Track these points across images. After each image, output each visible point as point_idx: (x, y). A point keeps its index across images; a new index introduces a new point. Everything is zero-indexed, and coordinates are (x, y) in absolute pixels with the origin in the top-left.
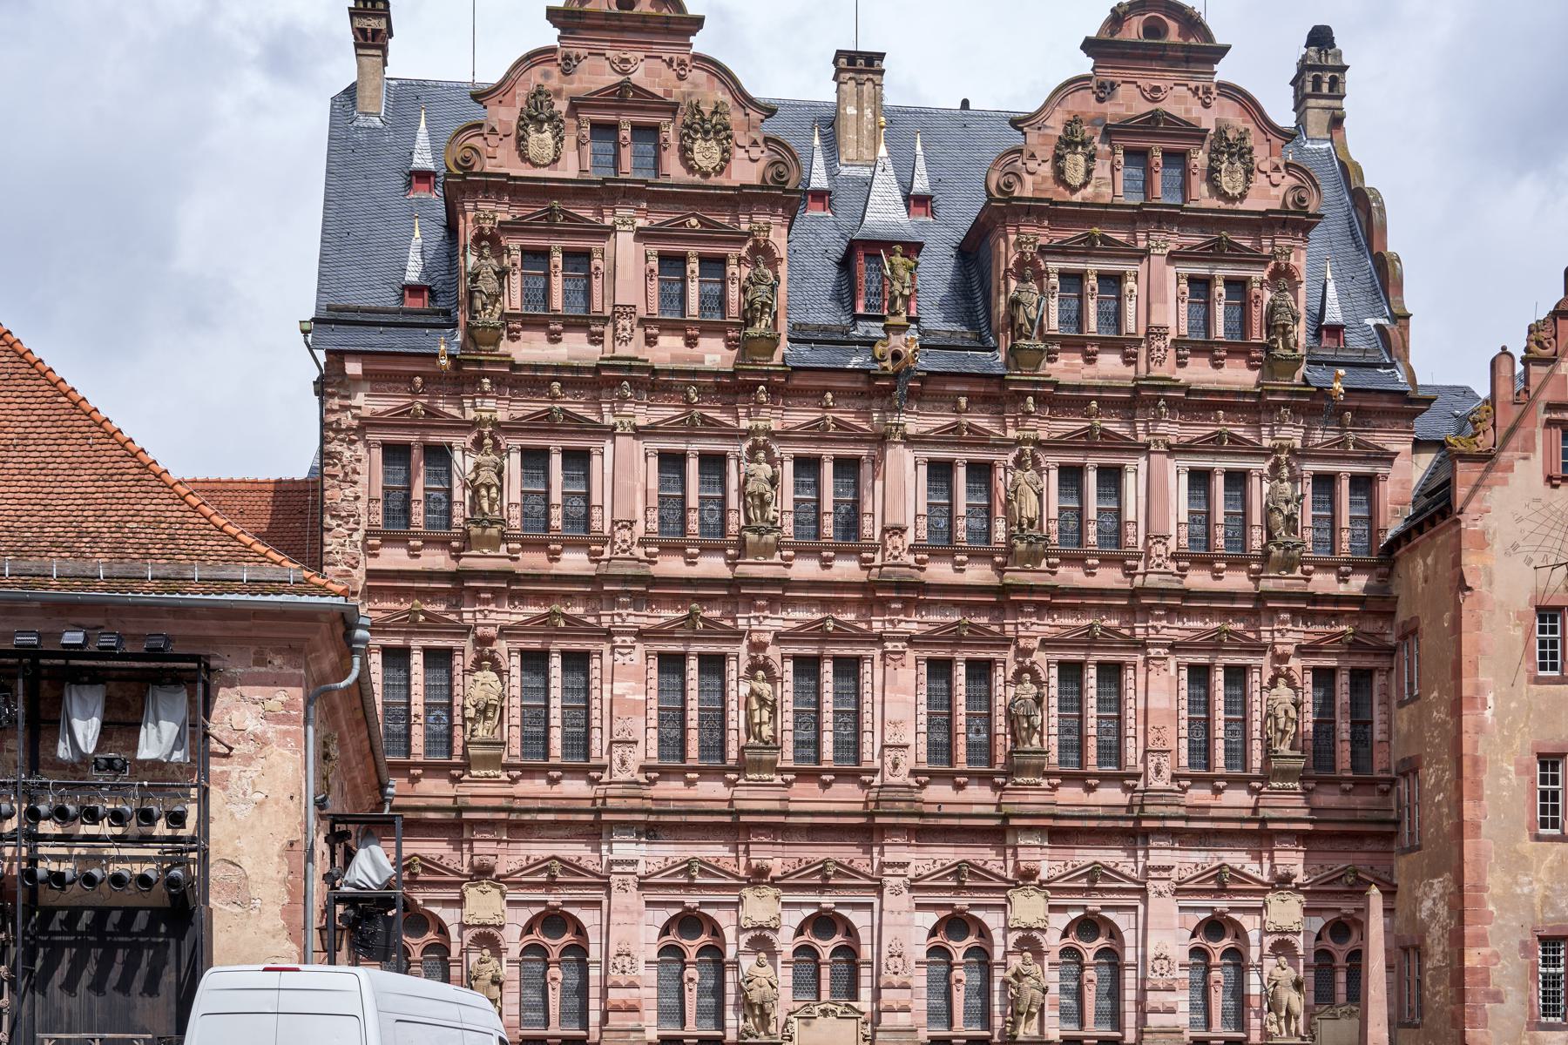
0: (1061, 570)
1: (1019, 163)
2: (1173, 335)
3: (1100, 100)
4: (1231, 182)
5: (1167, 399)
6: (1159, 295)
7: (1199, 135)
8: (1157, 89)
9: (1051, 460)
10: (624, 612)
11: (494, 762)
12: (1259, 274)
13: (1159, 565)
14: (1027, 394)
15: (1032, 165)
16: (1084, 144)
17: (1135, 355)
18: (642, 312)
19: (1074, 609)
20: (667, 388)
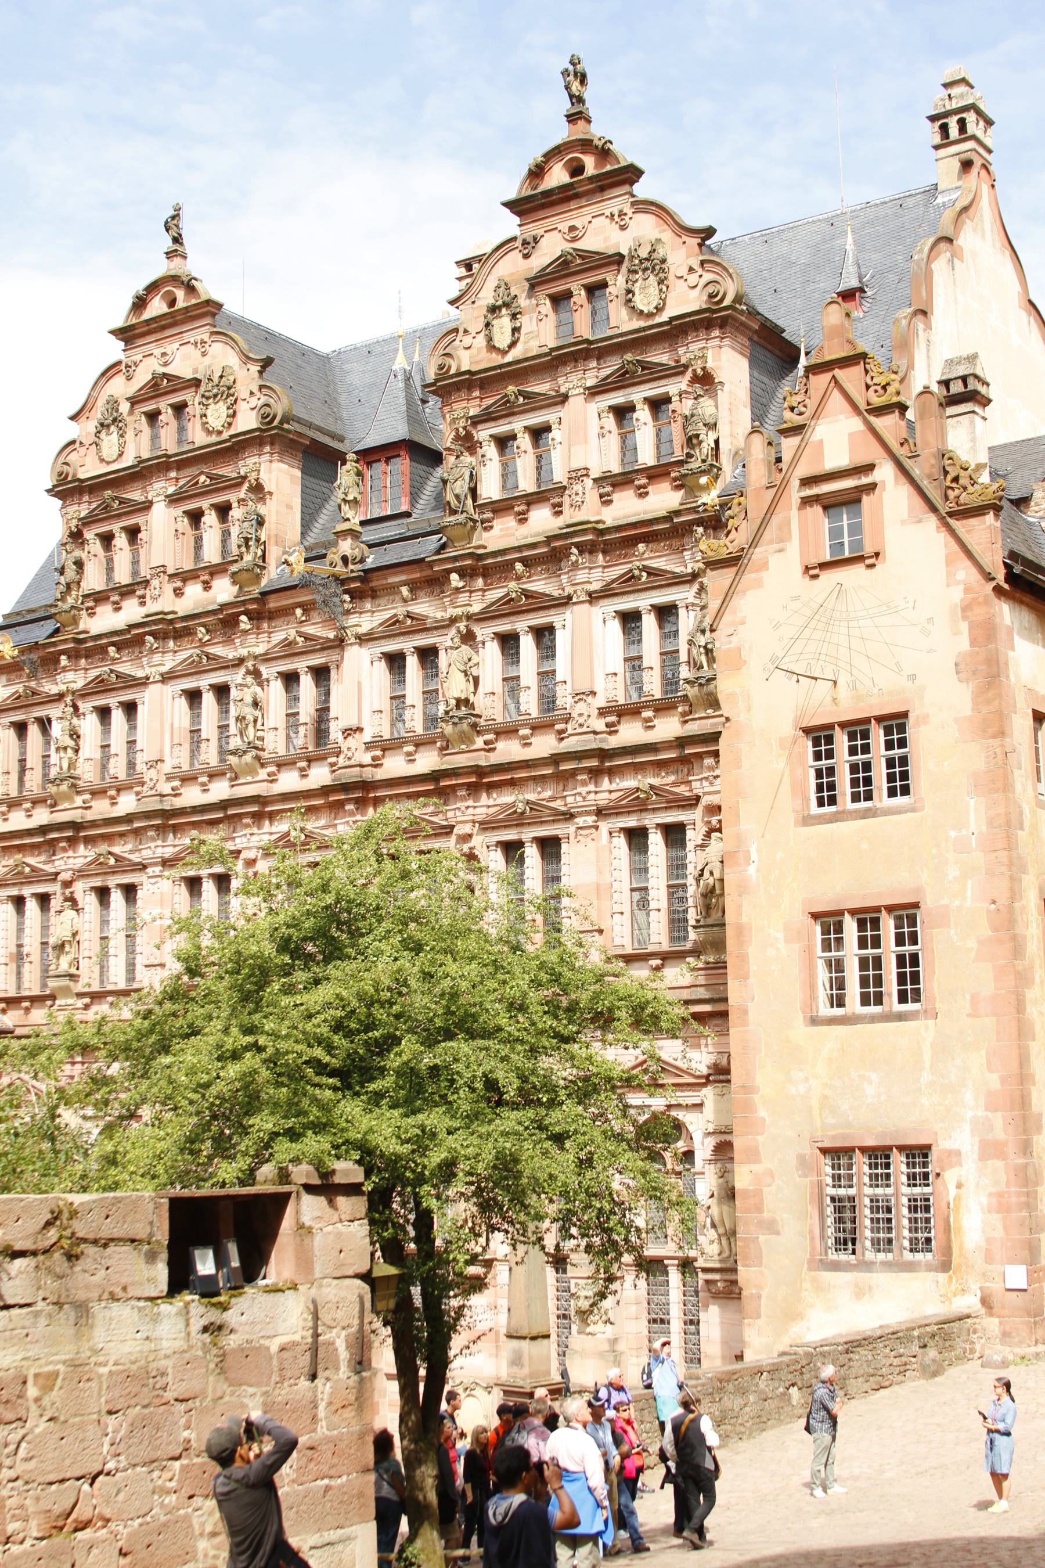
0: (501, 745)
1: (457, 342)
2: (595, 474)
3: (526, 256)
4: (646, 298)
5: (577, 545)
6: (584, 436)
7: (617, 259)
8: (572, 228)
9: (483, 632)
10: (152, 845)
11: (66, 991)
12: (673, 387)
13: (581, 725)
14: (449, 571)
15: (467, 340)
16: (506, 305)
17: (560, 505)
18: (171, 571)
19: (512, 783)
20: (187, 633)
